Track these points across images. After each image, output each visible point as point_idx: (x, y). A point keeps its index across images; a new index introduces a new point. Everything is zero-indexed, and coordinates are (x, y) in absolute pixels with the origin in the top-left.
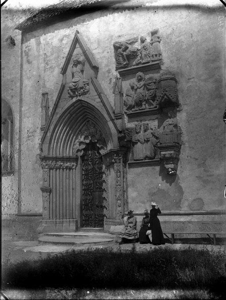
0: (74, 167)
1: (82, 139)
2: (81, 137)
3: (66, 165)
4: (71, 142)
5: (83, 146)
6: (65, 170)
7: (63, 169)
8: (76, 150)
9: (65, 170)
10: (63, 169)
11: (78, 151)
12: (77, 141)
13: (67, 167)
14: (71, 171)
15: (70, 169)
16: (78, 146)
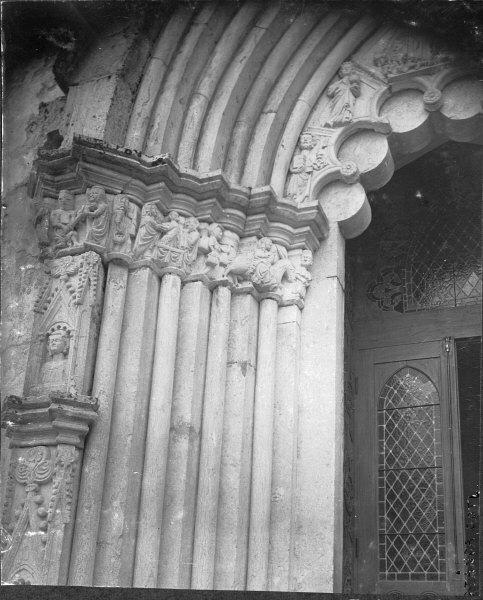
0: (288, 292)
1: (364, 109)
2: (356, 94)
3: (240, 262)
4: (279, 128)
5: (373, 154)
6: (224, 292)
7: (213, 288)
8: (319, 176)
9: (224, 292)
10: (213, 288)
11: (334, 181)
12: (325, 113)
13: (241, 276)
14: (269, 307)
15: (262, 293)
16: (331, 151)
